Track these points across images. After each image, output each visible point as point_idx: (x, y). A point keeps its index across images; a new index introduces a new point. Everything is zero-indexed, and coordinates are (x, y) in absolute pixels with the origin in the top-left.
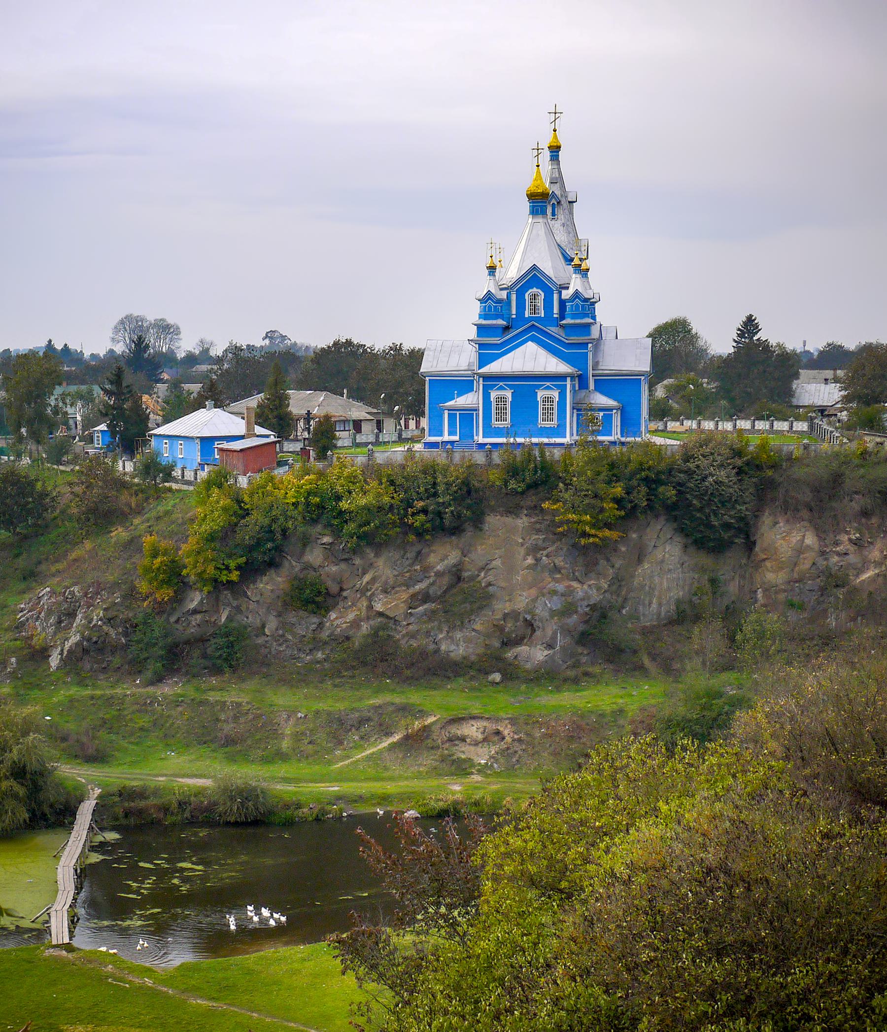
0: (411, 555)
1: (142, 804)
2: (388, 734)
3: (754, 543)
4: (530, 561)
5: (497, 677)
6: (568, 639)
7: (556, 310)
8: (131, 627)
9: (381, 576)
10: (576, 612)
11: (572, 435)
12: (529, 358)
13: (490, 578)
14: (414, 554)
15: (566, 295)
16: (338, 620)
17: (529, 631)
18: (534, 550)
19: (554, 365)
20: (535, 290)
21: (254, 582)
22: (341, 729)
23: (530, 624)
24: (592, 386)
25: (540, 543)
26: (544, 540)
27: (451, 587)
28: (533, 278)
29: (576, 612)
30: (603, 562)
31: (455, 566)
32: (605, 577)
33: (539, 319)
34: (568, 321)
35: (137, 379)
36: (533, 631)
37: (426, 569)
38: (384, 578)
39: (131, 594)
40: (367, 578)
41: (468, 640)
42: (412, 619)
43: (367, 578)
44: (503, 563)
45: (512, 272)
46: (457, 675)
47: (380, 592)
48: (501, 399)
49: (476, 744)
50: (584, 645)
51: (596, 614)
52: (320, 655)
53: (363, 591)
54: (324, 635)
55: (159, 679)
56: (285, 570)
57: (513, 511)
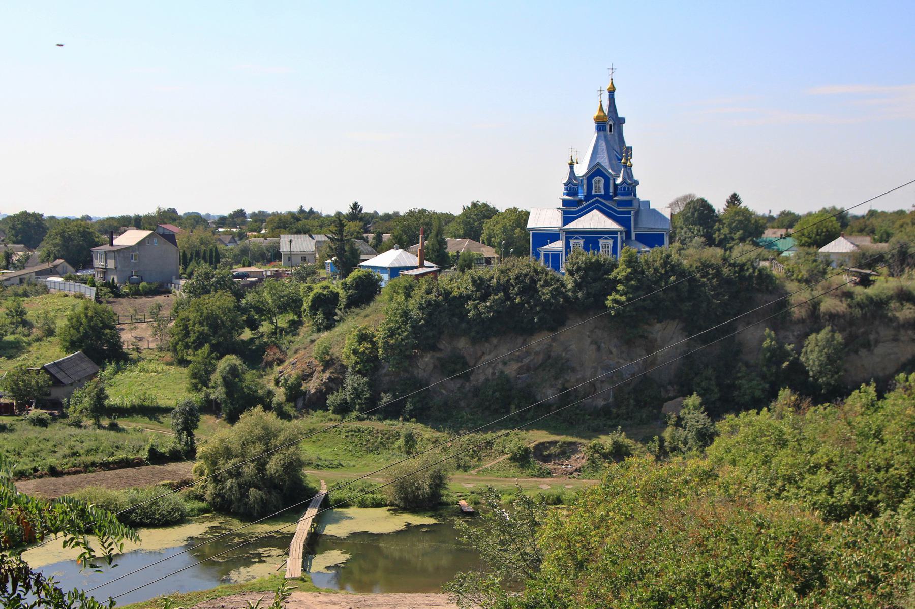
7: (611, 190)
12: (595, 220)
19: (610, 225)
20: (598, 177)
24: (633, 237)
33: (600, 196)
35: (352, 232)
48: (575, 245)
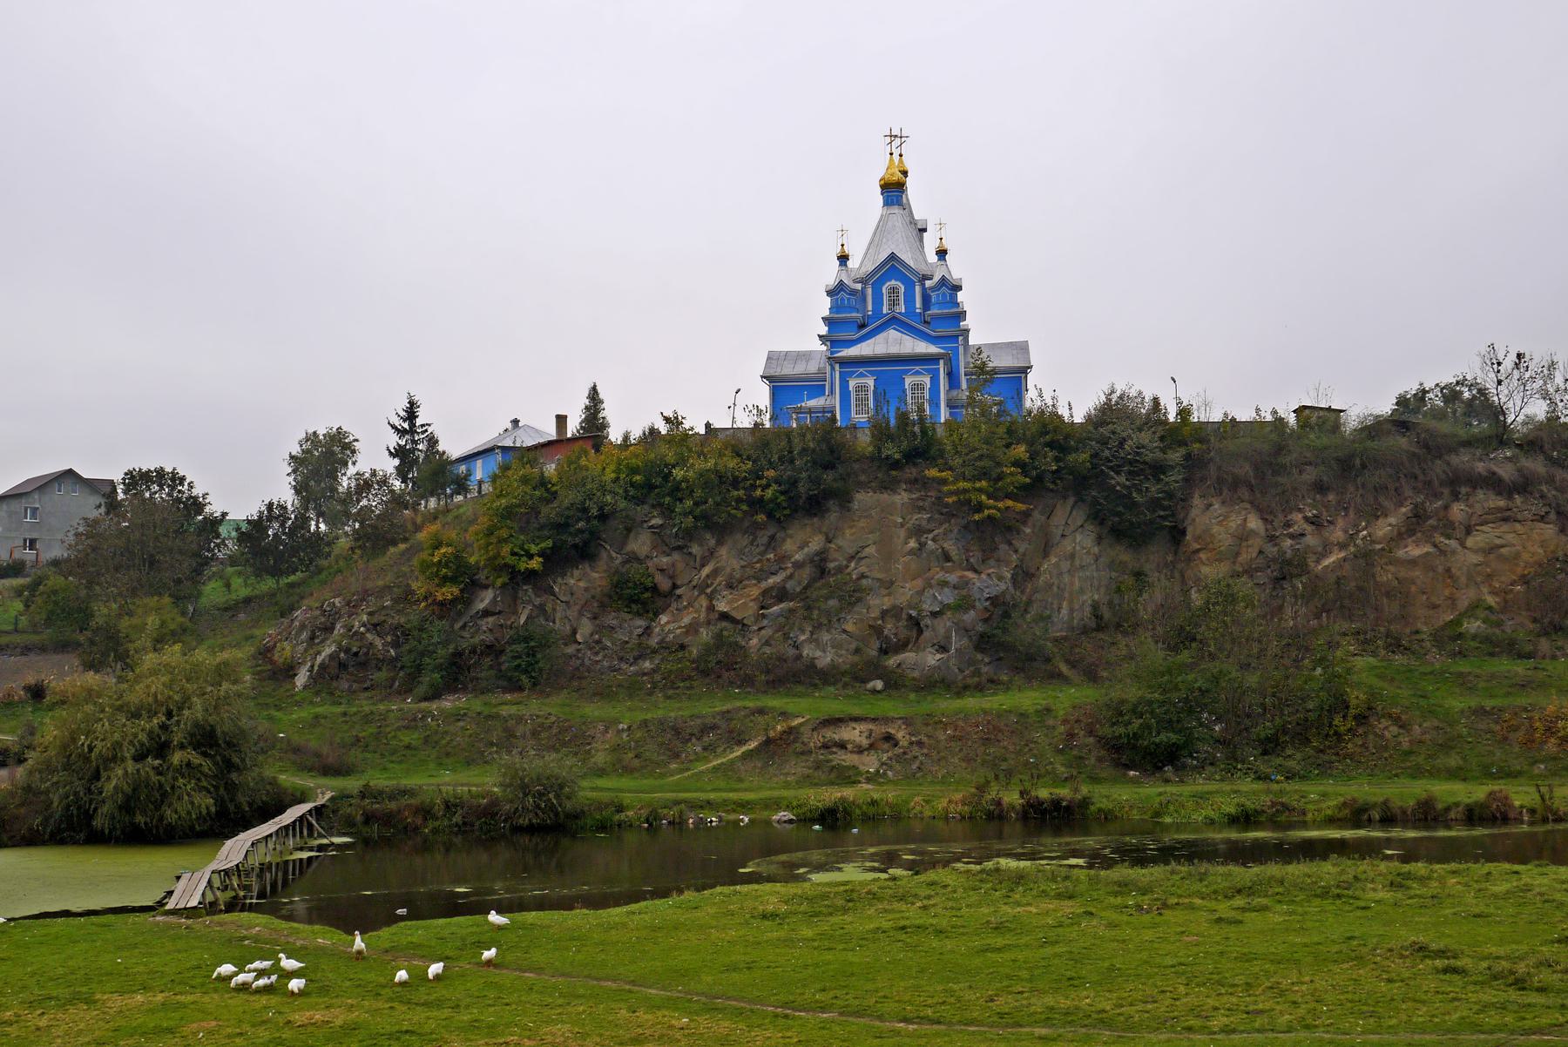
0: (763, 539)
1: (393, 806)
2: (740, 743)
3: (1183, 532)
4: (913, 544)
5: (879, 685)
6: (965, 641)
7: (918, 304)
8: (401, 635)
9: (723, 568)
10: (974, 607)
13: (863, 569)
14: (765, 540)
16: (667, 624)
17: (914, 634)
18: (918, 532)
19: (923, 348)
20: (893, 282)
21: (563, 575)
22: (676, 739)
23: (916, 624)
25: (924, 523)
26: (929, 520)
27: (812, 581)
28: (892, 266)
29: (974, 607)
30: (1003, 547)
31: (818, 554)
32: (1007, 563)
34: (934, 311)
36: (920, 632)
37: (782, 559)
38: (728, 570)
39: (407, 597)
40: (706, 571)
41: (837, 646)
42: (765, 622)
43: (706, 571)
44: (878, 551)
46: (826, 682)
47: (725, 587)
48: (861, 388)
49: (860, 750)
50: (983, 651)
51: (999, 611)
52: (647, 665)
53: (701, 588)
54: (653, 642)
55: (435, 695)
56: (602, 564)
57: (889, 486)
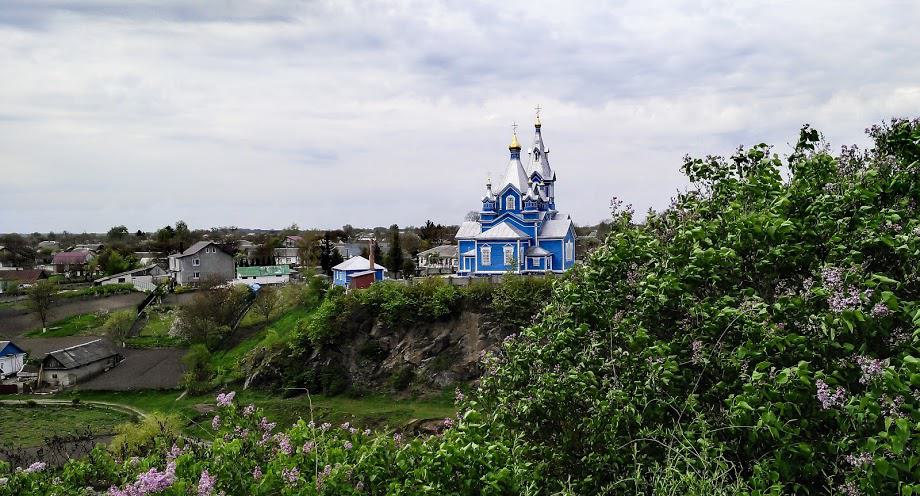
0: (423, 331)
11: (548, 267)
12: (502, 230)
15: (524, 198)
24: (537, 243)
28: (510, 190)
34: (526, 211)
45: (498, 188)
47: (406, 353)
